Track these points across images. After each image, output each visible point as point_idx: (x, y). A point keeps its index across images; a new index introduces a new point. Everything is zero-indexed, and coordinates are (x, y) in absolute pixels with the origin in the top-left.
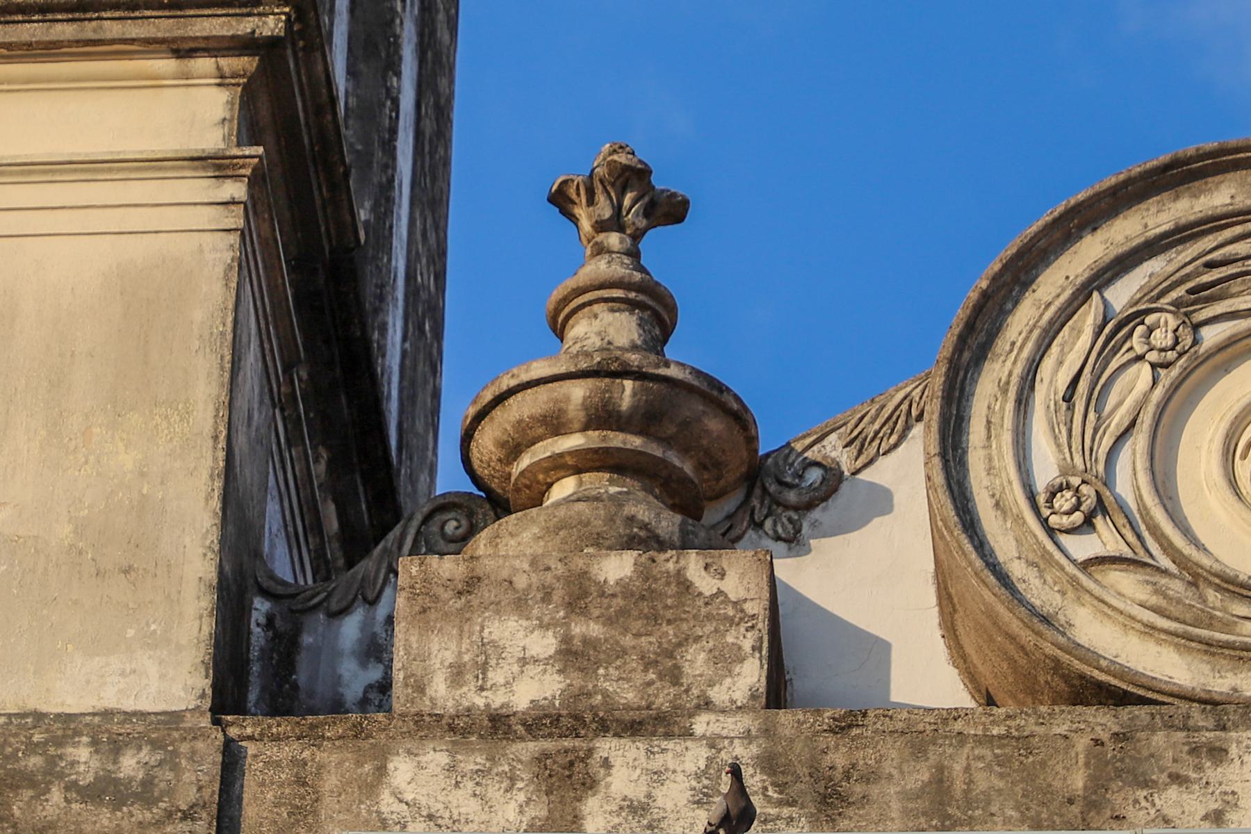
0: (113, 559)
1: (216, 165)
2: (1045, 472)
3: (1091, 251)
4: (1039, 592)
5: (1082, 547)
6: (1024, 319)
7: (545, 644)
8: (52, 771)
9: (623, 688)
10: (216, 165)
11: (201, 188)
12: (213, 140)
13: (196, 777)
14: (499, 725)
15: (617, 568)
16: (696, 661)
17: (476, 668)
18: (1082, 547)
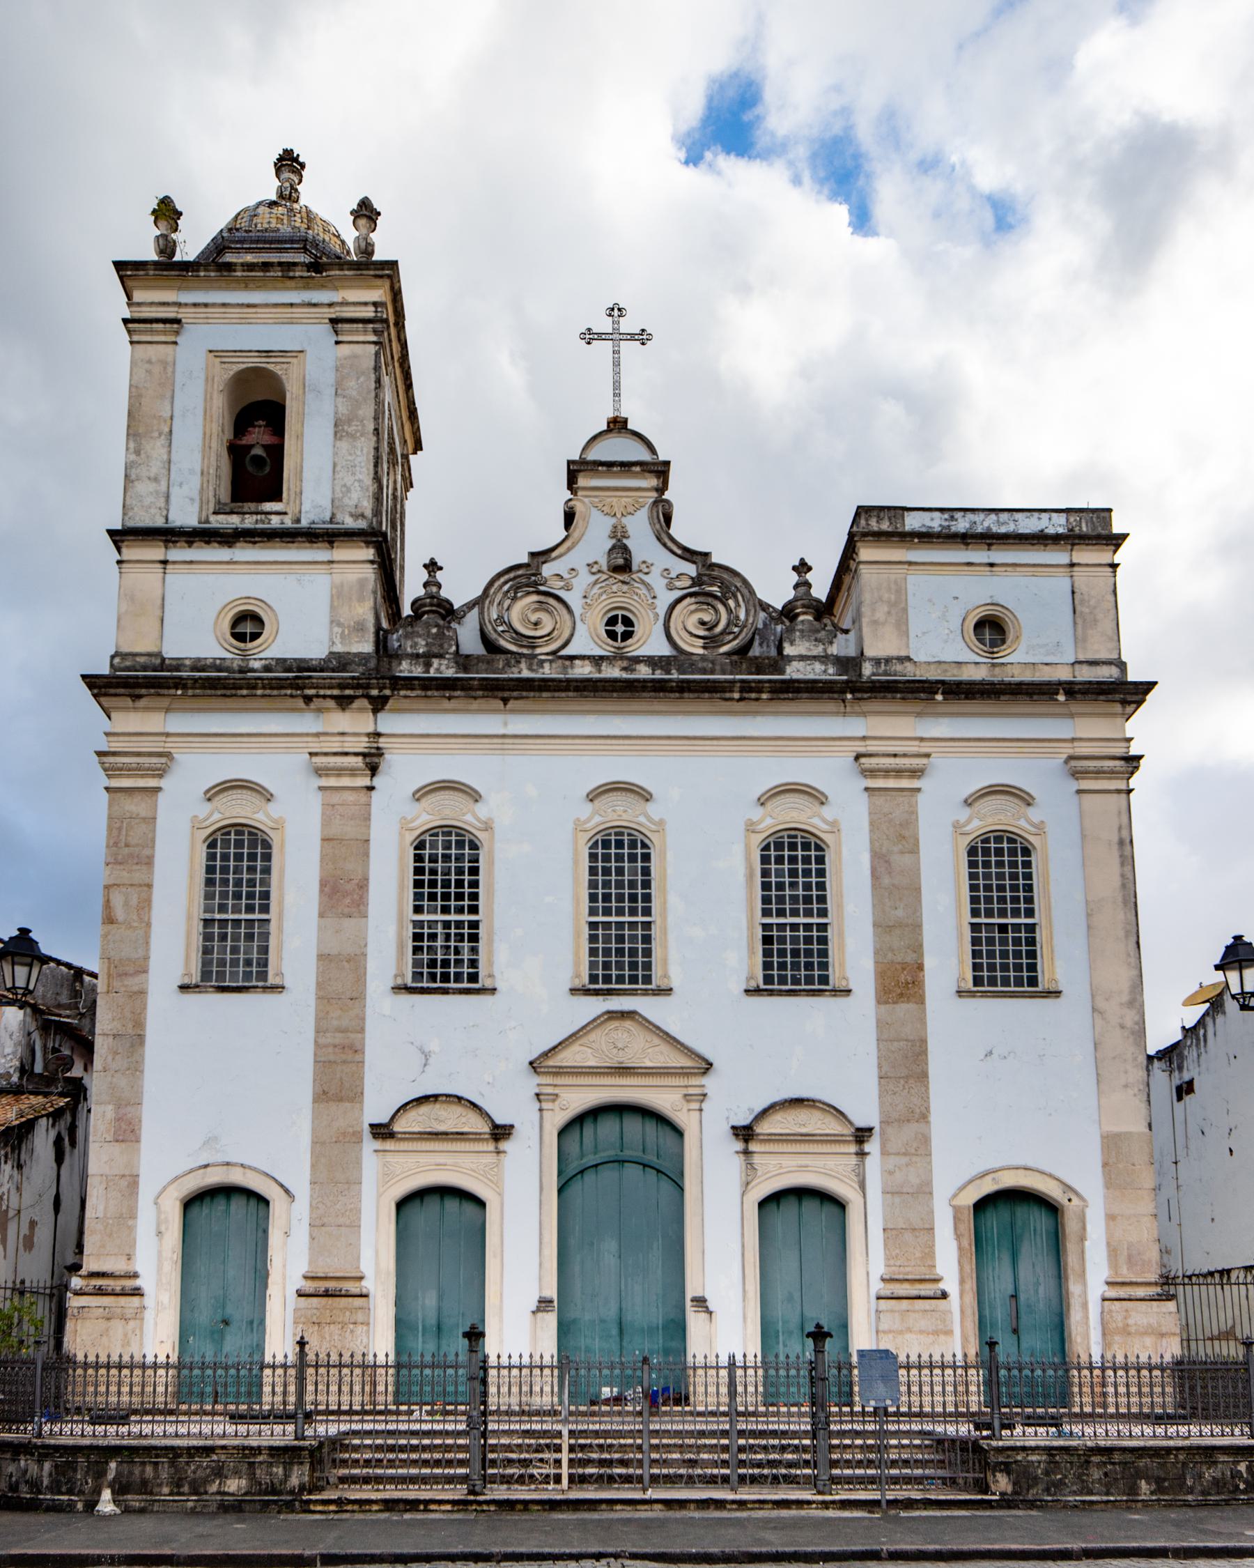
0: (359, 627)
1: (372, 562)
2: (495, 617)
3: (502, 580)
4: (494, 636)
5: (500, 629)
6: (492, 591)
7: (423, 643)
8: (354, 662)
9: (435, 650)
10: (372, 562)
11: (369, 566)
12: (371, 558)
13: (372, 664)
14: (418, 656)
15: (434, 630)
16: (446, 646)
17: (415, 645)
18: (500, 629)
